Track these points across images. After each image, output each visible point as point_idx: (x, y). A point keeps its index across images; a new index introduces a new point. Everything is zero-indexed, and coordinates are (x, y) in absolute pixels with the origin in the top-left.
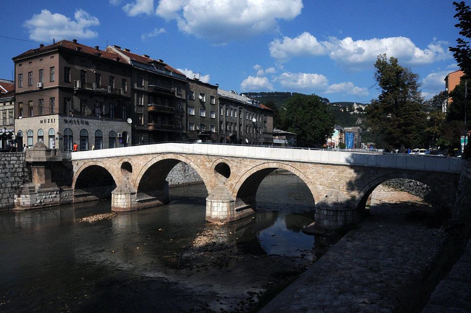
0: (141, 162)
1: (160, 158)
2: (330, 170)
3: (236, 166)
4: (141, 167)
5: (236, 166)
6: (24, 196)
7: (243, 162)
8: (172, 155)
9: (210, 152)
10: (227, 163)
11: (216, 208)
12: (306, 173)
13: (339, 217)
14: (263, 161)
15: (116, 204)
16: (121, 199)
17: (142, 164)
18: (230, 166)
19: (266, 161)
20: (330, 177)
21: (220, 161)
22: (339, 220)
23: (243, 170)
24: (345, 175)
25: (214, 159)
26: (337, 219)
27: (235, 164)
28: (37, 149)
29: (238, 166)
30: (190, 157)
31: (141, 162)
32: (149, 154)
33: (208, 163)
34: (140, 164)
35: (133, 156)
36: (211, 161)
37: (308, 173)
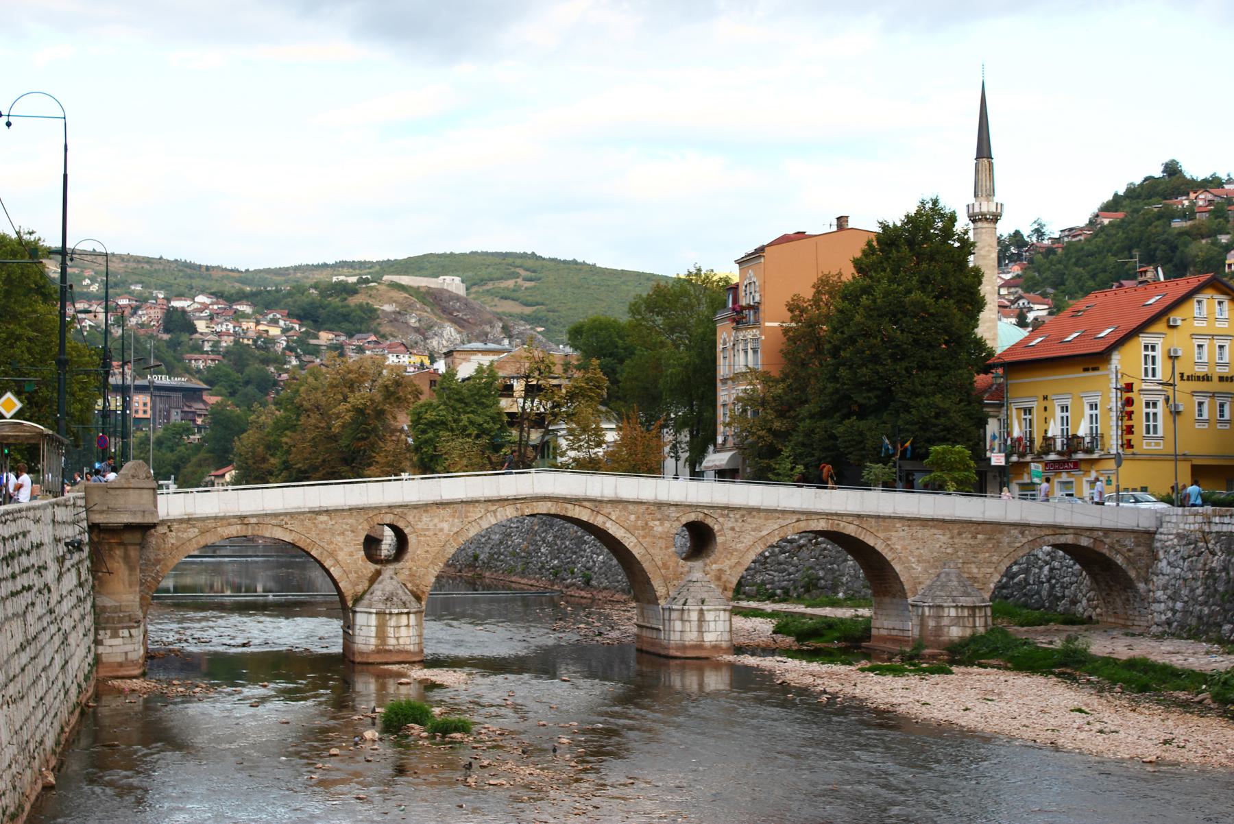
0: (445, 526)
1: (510, 512)
2: (936, 531)
3: (733, 529)
4: (443, 537)
5: (733, 529)
6: (126, 633)
7: (749, 520)
8: (549, 504)
9: (663, 497)
10: (709, 521)
11: (712, 625)
12: (889, 539)
13: (977, 619)
14: (795, 518)
15: (392, 641)
16: (408, 626)
17: (446, 531)
18: (716, 528)
19: (803, 517)
20: (938, 546)
21: (692, 517)
22: (977, 624)
23: (748, 540)
24: (965, 541)
25: (673, 513)
26: (974, 621)
27: (730, 525)
28: (134, 482)
29: (737, 529)
30: (607, 509)
31: (445, 526)
32: (478, 501)
33: (657, 523)
34: (441, 530)
35: (416, 507)
36: (668, 518)
37: (894, 540)
